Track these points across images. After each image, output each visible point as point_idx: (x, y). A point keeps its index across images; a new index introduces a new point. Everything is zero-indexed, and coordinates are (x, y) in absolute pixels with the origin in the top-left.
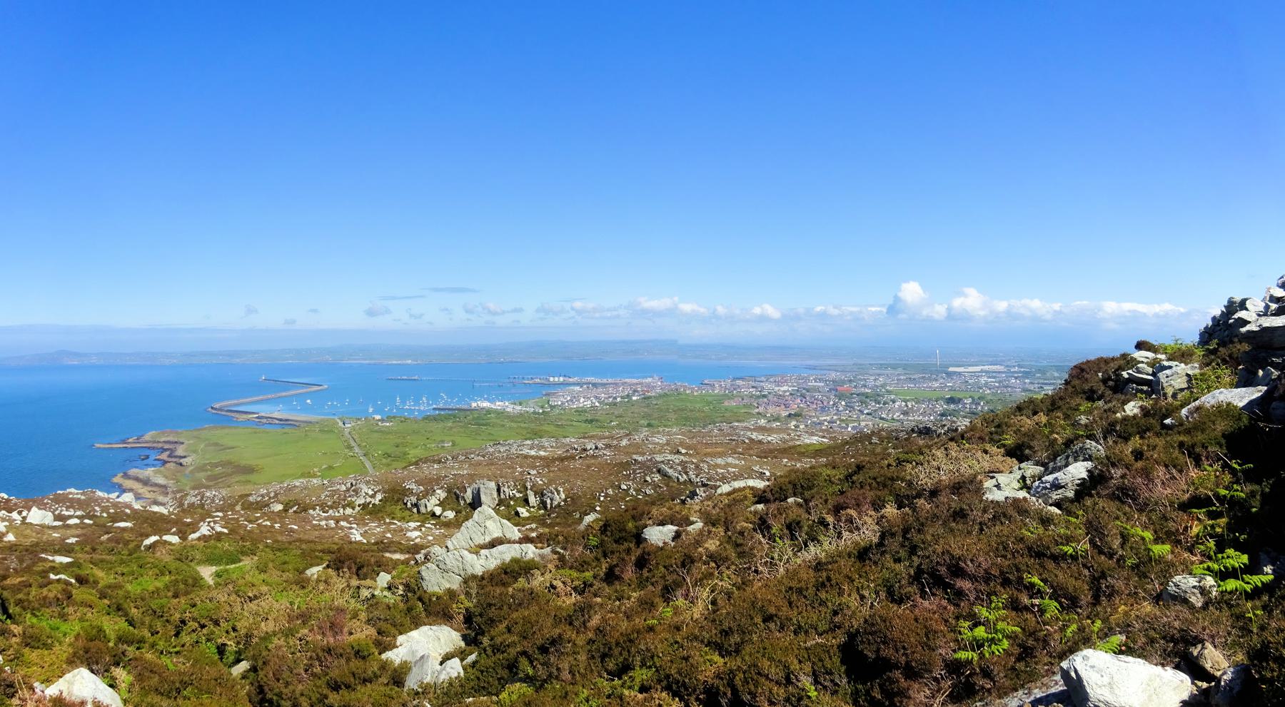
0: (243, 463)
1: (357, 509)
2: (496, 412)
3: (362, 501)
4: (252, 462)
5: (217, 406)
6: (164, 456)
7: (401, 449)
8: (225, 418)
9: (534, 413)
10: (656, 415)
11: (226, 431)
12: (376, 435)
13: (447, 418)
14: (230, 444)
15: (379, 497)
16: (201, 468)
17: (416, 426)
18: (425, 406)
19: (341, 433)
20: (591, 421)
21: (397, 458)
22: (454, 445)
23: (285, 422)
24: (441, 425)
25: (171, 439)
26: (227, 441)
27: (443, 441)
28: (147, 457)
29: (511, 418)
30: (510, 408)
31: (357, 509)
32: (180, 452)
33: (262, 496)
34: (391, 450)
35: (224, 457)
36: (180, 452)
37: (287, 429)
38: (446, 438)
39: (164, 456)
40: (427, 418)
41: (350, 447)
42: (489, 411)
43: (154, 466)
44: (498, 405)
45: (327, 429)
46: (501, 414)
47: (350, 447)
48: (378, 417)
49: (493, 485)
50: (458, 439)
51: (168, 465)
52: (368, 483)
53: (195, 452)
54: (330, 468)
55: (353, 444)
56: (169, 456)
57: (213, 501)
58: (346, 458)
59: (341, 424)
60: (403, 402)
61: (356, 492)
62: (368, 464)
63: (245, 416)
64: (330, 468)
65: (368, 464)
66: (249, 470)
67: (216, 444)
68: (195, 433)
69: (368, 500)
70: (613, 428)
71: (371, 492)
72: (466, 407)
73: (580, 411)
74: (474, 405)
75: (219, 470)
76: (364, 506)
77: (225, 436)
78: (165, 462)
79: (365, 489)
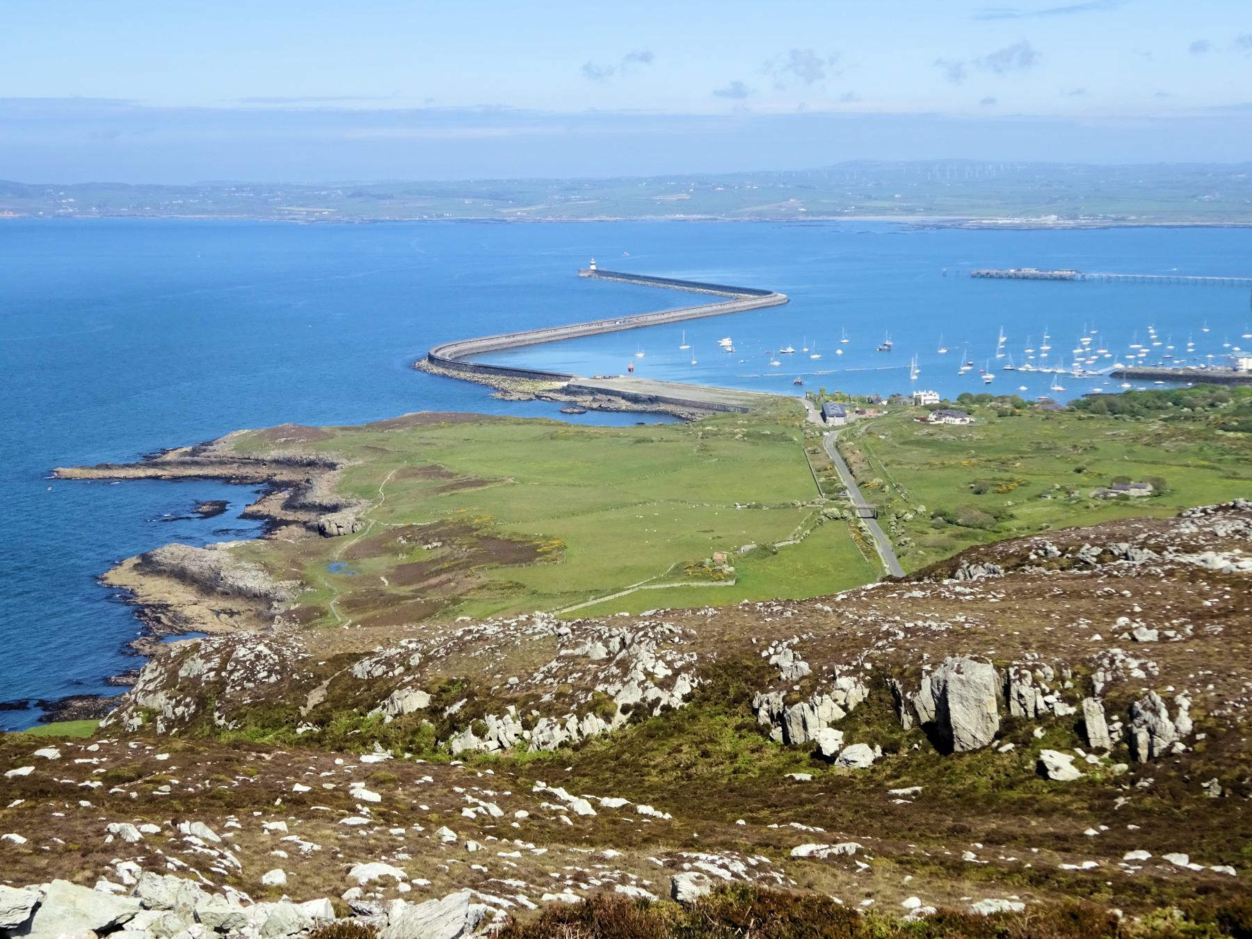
0: (507, 529)
1: (620, 718)
3: (631, 696)
4: (534, 529)
5: (446, 353)
6: (273, 506)
7: (989, 501)
8: (473, 385)
11: (468, 430)
12: (916, 454)
13: (1152, 405)
14: (475, 470)
15: (684, 685)
16: (379, 545)
17: (1047, 429)
18: (1089, 366)
22: (1158, 493)
23: (646, 407)
24: (1127, 427)
25: (295, 452)
26: (464, 464)
27: (1124, 481)
28: (220, 508)
31: (620, 718)
32: (321, 492)
33: (389, 663)
35: (451, 510)
36: (321, 492)
37: (652, 429)
38: (1145, 471)
39: (273, 506)
40: (1088, 406)
43: (239, 533)
45: (769, 430)
47: (833, 491)
49: (985, 674)
50: (1173, 475)
51: (281, 534)
52: (664, 640)
53: (367, 493)
54: (765, 551)
55: (844, 479)
56: (288, 505)
57: (251, 674)
59: (814, 417)
60: (1015, 345)
61: (625, 666)
63: (528, 386)
66: (523, 552)
67: (433, 471)
68: (372, 437)
69: (653, 693)
71: (662, 671)
72: (1219, 370)
75: (430, 551)
76: (638, 712)
77: (465, 449)
78: (273, 524)
79: (646, 658)
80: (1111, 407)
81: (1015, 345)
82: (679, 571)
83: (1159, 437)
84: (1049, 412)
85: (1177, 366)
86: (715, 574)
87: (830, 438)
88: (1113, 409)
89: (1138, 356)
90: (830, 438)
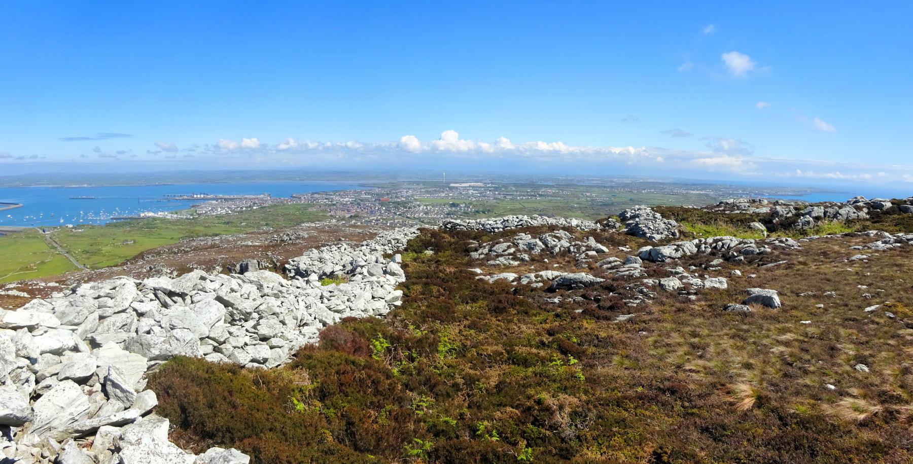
2: (159, 219)
7: (94, 247)
9: (187, 219)
10: (270, 218)
13: (123, 225)
18: (104, 217)
19: (44, 239)
20: (228, 223)
21: (94, 253)
22: (135, 242)
27: (127, 241)
29: (170, 222)
30: (169, 217)
34: (88, 248)
38: (129, 239)
40: (108, 225)
41: (55, 248)
42: (154, 219)
44: (160, 214)
46: (163, 220)
47: (55, 248)
48: (71, 226)
50: (136, 238)
54: (43, 263)
55: (55, 245)
58: (53, 255)
59: (41, 232)
60: (86, 214)
62: (72, 259)
64: (43, 263)
65: (72, 259)
70: (243, 227)
72: (136, 216)
73: (219, 217)
74: (142, 215)
80: (115, 226)
81: (86, 214)
82: (21, 269)
83: (130, 231)
84: (101, 227)
85: (125, 216)
86: (31, 269)
87: (48, 237)
88: (115, 226)
89: (116, 215)
90: (48, 237)
